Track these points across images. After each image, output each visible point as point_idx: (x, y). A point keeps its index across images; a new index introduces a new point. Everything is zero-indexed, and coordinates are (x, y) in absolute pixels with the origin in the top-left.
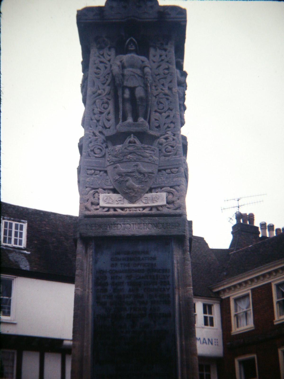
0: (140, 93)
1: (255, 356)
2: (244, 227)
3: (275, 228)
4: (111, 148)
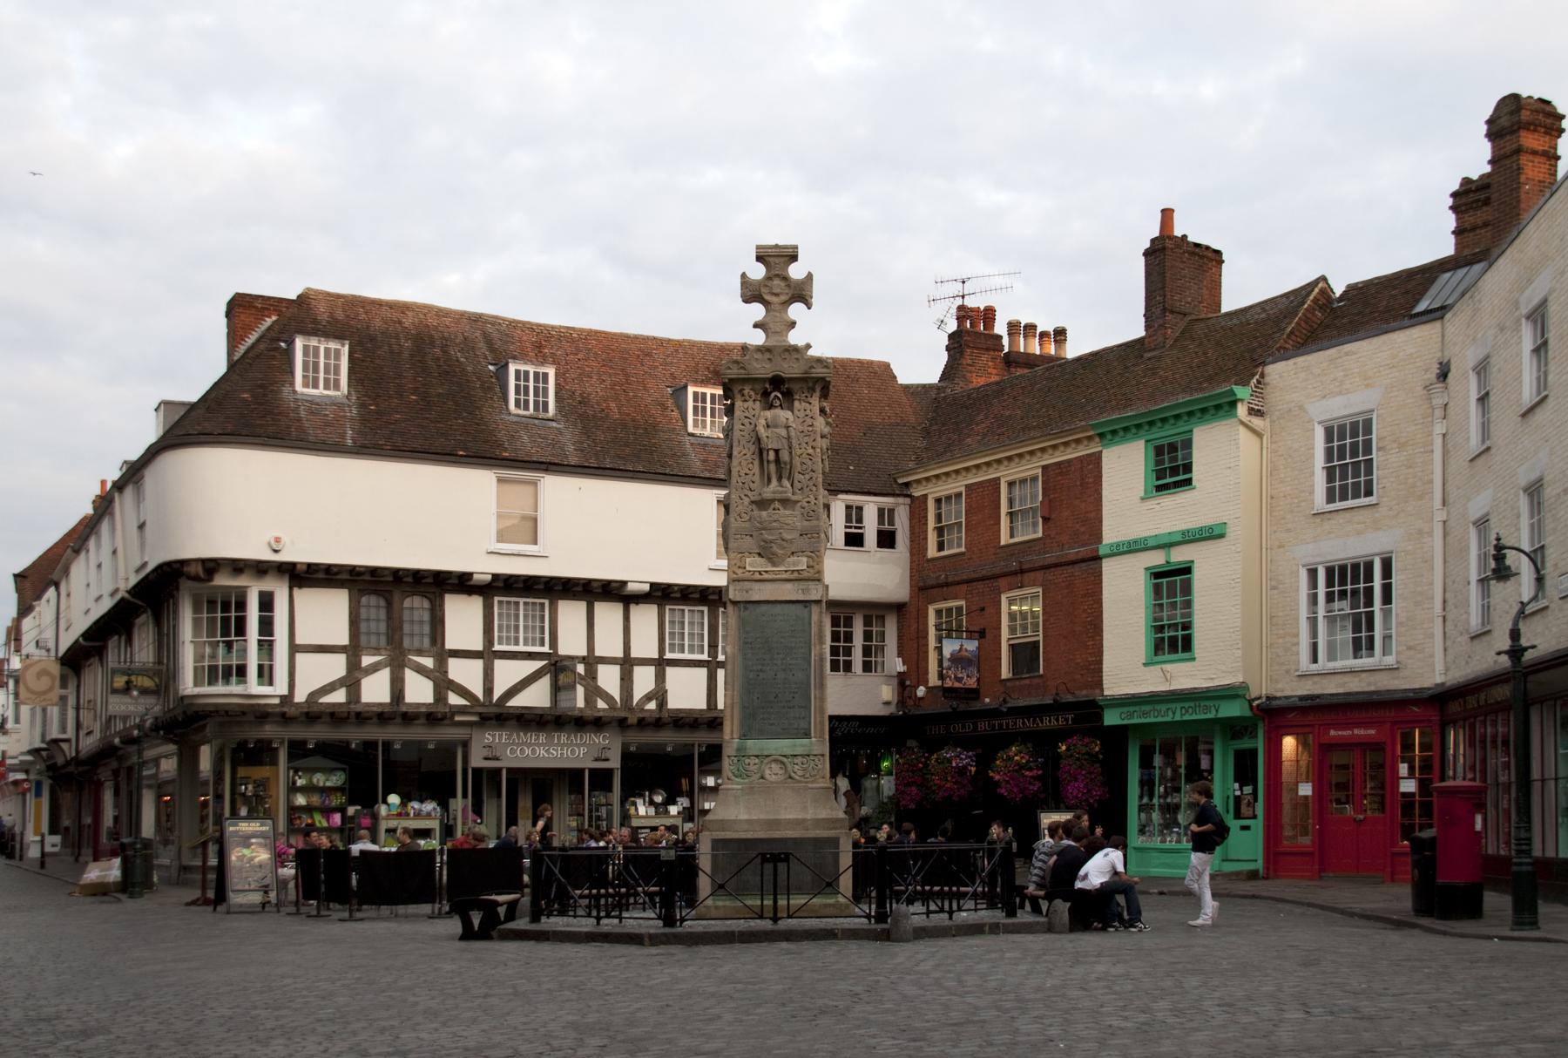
0: (785, 456)
1: (963, 603)
2: (972, 334)
3: (1039, 330)
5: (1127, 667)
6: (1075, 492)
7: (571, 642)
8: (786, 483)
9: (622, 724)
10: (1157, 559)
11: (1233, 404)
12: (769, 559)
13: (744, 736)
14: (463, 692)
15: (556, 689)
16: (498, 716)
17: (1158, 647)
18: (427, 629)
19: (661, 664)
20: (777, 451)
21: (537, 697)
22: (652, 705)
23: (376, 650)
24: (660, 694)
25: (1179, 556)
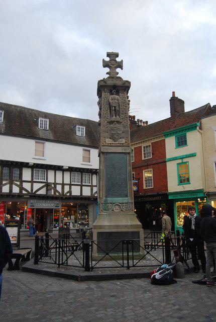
0: (117, 108)
4: (109, 125)
5: (173, 186)
6: (159, 148)
7: (51, 179)
8: (118, 117)
9: (62, 198)
10: (180, 161)
11: (196, 127)
12: (113, 140)
13: (106, 197)
14: (26, 190)
15: (47, 190)
16: (34, 196)
17: (181, 182)
18: (18, 176)
19: (70, 185)
20: (115, 107)
21: (43, 192)
22: (68, 194)
23: (6, 180)
24: (70, 192)
25: (185, 160)
